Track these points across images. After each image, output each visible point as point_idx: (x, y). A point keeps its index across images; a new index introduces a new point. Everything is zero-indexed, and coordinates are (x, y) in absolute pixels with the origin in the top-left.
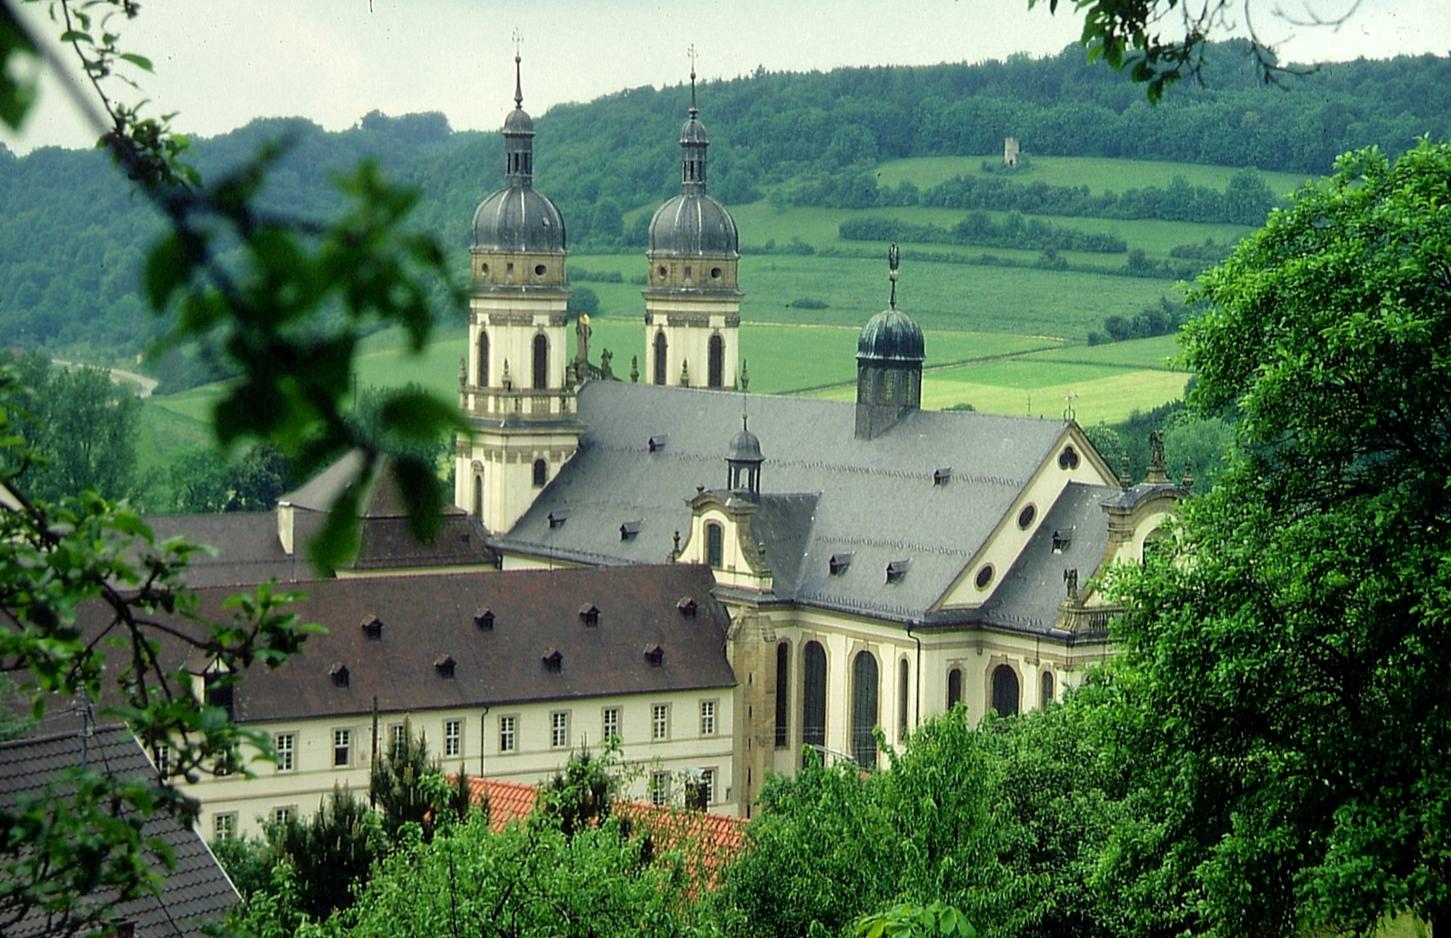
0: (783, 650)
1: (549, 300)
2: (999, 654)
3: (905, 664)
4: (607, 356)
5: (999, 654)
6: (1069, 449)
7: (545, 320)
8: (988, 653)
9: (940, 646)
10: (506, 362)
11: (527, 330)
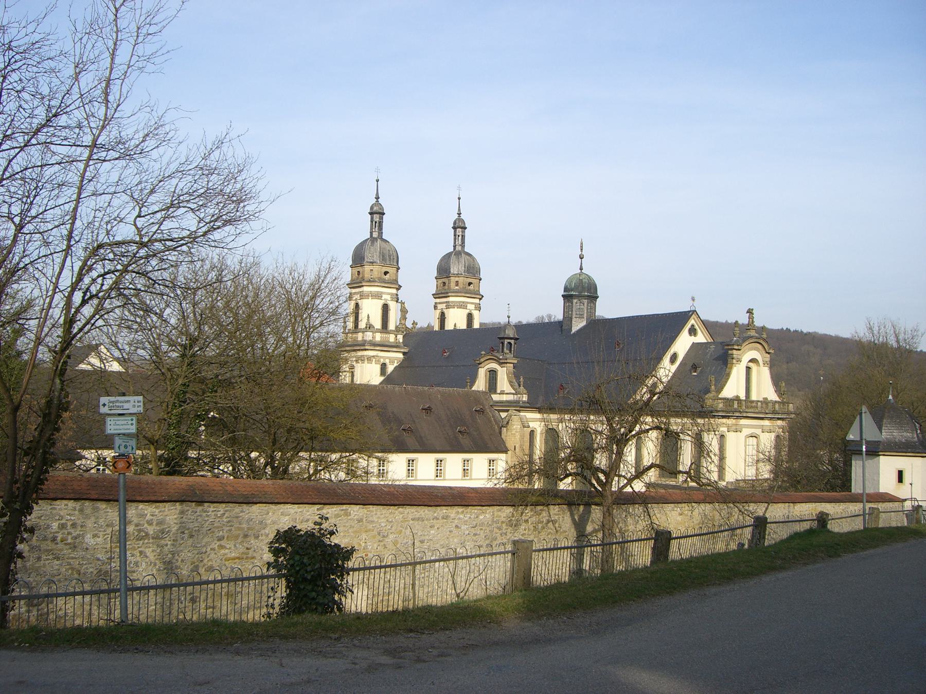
4: (414, 323)
6: (693, 326)
7: (388, 297)
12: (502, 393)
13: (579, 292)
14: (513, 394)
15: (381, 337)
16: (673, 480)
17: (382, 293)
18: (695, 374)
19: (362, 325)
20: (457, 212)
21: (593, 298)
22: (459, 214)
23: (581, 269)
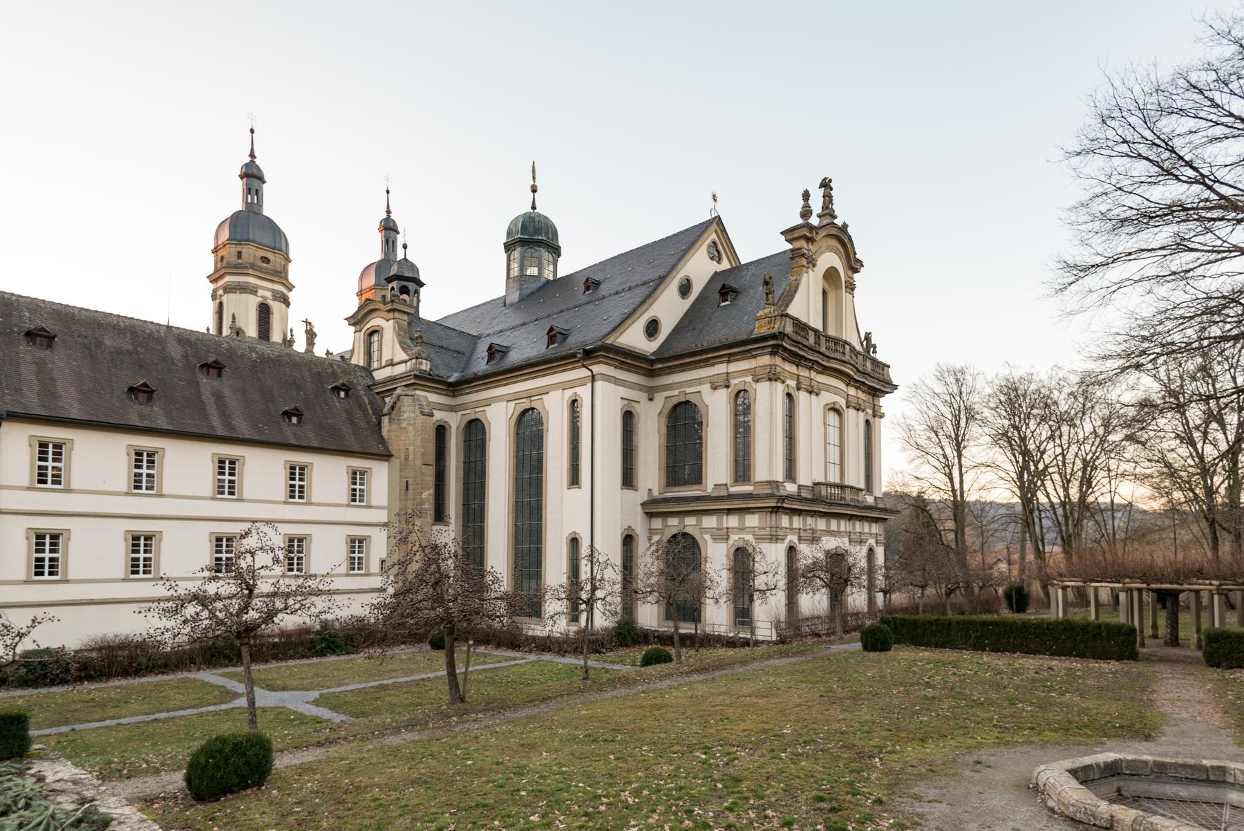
0: (441, 431)
1: (272, 281)
2: (676, 392)
5: (676, 392)
7: (269, 294)
8: (660, 398)
10: (234, 315)
11: (251, 297)
12: (391, 364)
13: (529, 235)
14: (406, 362)
16: (695, 487)
18: (727, 303)
21: (556, 251)
22: (388, 212)
23: (534, 208)
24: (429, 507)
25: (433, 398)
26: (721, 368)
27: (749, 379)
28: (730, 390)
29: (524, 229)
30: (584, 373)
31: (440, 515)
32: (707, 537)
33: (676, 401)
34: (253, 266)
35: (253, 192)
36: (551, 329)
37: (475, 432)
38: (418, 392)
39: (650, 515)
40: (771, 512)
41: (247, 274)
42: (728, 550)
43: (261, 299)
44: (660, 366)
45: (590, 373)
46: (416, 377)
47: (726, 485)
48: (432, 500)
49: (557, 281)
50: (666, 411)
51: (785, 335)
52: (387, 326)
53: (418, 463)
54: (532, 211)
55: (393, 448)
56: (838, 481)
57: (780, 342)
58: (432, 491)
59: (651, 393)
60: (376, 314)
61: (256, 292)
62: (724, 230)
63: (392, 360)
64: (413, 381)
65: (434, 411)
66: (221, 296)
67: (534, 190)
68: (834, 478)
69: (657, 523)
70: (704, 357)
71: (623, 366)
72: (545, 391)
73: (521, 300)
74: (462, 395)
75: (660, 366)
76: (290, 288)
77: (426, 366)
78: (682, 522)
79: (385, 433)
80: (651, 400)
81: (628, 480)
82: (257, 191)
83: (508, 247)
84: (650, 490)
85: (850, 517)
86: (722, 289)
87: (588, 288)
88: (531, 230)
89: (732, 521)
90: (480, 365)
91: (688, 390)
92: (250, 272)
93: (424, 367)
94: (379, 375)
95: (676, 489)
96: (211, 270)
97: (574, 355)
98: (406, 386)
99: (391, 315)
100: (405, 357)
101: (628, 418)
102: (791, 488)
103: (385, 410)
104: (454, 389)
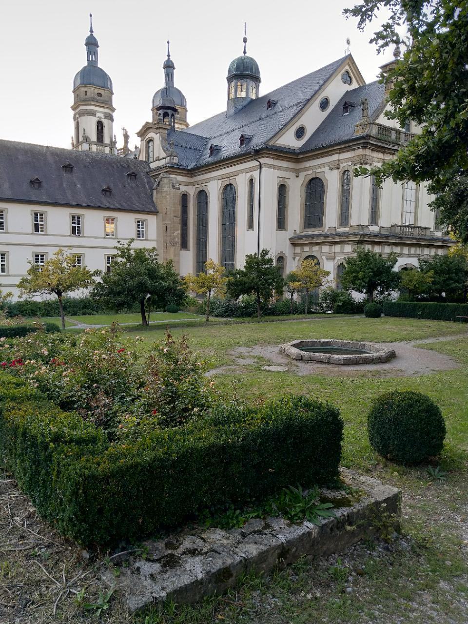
0: (185, 197)
1: (103, 107)
3: (251, 181)
7: (102, 115)
8: (302, 175)
9: (274, 167)
13: (241, 72)
14: (165, 158)
15: (97, 149)
16: (319, 229)
17: (96, 111)
18: (348, 113)
19: (81, 139)
20: (167, 54)
21: (256, 79)
23: (245, 52)
24: (178, 240)
25: (180, 178)
26: (335, 157)
27: (350, 163)
28: (340, 170)
29: (238, 68)
30: (254, 163)
31: (184, 245)
32: (324, 258)
33: (311, 177)
34: (93, 99)
35: (92, 53)
36: (242, 136)
37: (202, 196)
38: (171, 176)
39: (295, 245)
40: (358, 243)
41: (91, 105)
42: (334, 265)
43: (98, 118)
44: (302, 156)
45: (259, 163)
46: (170, 167)
47: (335, 227)
48: (180, 236)
49: (258, 99)
50: (306, 183)
51: (370, 136)
52: (156, 137)
53: (172, 216)
54: (244, 55)
55: (159, 208)
56: (412, 223)
57: (368, 141)
58: (180, 232)
59: (297, 172)
60: (151, 130)
61: (95, 114)
62: (354, 63)
63: (159, 157)
64: (168, 170)
65: (181, 186)
66: (78, 118)
67: (245, 40)
68: (409, 220)
69: (298, 250)
70: (326, 150)
71: (279, 158)
72: (236, 174)
73: (236, 113)
74: (195, 176)
75: (302, 156)
76: (113, 110)
77: (176, 160)
78: (311, 249)
79: (154, 199)
80: (297, 177)
81: (281, 224)
82: (94, 53)
83: (230, 79)
84: (295, 231)
85: (419, 246)
86: (344, 105)
87: (269, 106)
88: (242, 68)
89: (337, 248)
90: (207, 158)
91: (318, 171)
92: (92, 103)
93: (174, 161)
94: (153, 166)
95: (308, 230)
96: (72, 104)
97: (249, 153)
98: (165, 172)
99: (158, 131)
100: (165, 156)
101: (282, 189)
102: (374, 229)
103: (154, 187)
104: (191, 172)
